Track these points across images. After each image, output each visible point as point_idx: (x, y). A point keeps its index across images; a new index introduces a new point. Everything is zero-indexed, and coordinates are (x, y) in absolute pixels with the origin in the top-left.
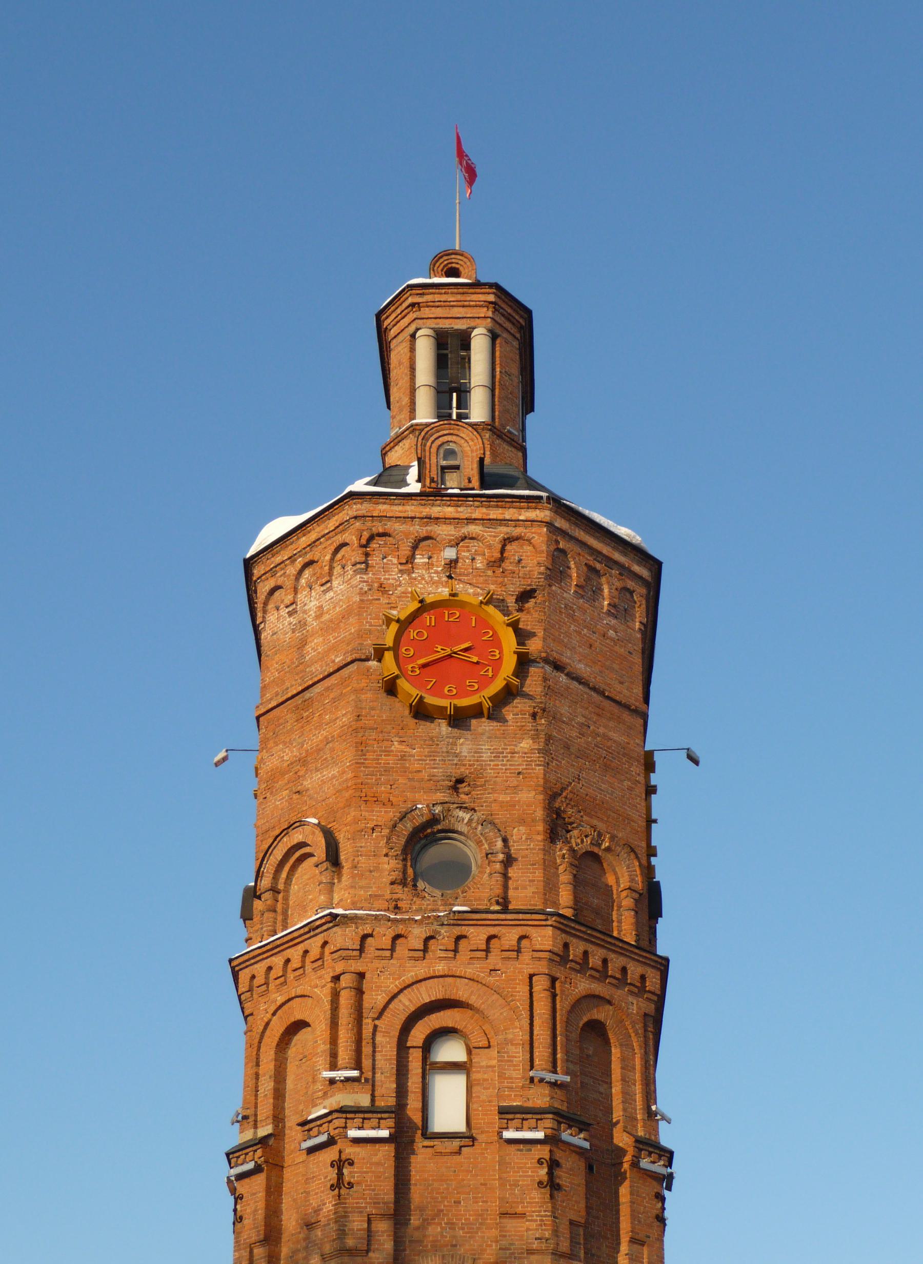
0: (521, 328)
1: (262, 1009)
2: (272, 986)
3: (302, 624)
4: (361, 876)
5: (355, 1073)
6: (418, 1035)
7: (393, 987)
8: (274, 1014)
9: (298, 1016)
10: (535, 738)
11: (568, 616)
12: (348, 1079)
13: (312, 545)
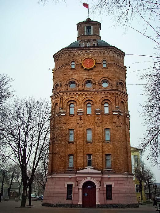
6: (69, 104)
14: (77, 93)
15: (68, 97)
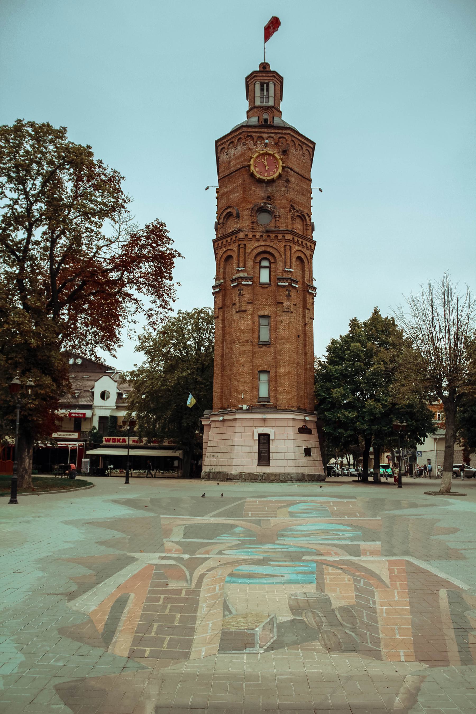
0: (280, 82)
1: (220, 252)
2: (223, 247)
3: (230, 157)
4: (244, 220)
5: (243, 268)
7: (252, 248)
8: (223, 253)
9: (230, 254)
10: (286, 187)
11: (294, 157)
12: (241, 271)
13: (233, 138)
14: (276, 236)
15: (259, 244)
